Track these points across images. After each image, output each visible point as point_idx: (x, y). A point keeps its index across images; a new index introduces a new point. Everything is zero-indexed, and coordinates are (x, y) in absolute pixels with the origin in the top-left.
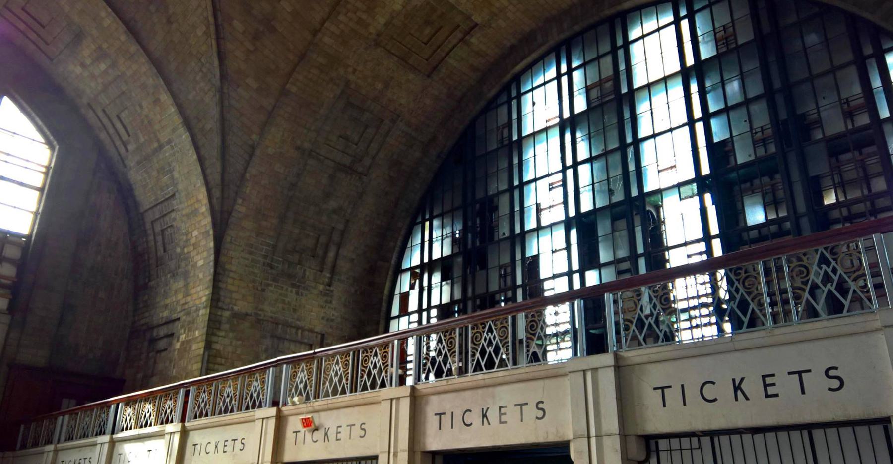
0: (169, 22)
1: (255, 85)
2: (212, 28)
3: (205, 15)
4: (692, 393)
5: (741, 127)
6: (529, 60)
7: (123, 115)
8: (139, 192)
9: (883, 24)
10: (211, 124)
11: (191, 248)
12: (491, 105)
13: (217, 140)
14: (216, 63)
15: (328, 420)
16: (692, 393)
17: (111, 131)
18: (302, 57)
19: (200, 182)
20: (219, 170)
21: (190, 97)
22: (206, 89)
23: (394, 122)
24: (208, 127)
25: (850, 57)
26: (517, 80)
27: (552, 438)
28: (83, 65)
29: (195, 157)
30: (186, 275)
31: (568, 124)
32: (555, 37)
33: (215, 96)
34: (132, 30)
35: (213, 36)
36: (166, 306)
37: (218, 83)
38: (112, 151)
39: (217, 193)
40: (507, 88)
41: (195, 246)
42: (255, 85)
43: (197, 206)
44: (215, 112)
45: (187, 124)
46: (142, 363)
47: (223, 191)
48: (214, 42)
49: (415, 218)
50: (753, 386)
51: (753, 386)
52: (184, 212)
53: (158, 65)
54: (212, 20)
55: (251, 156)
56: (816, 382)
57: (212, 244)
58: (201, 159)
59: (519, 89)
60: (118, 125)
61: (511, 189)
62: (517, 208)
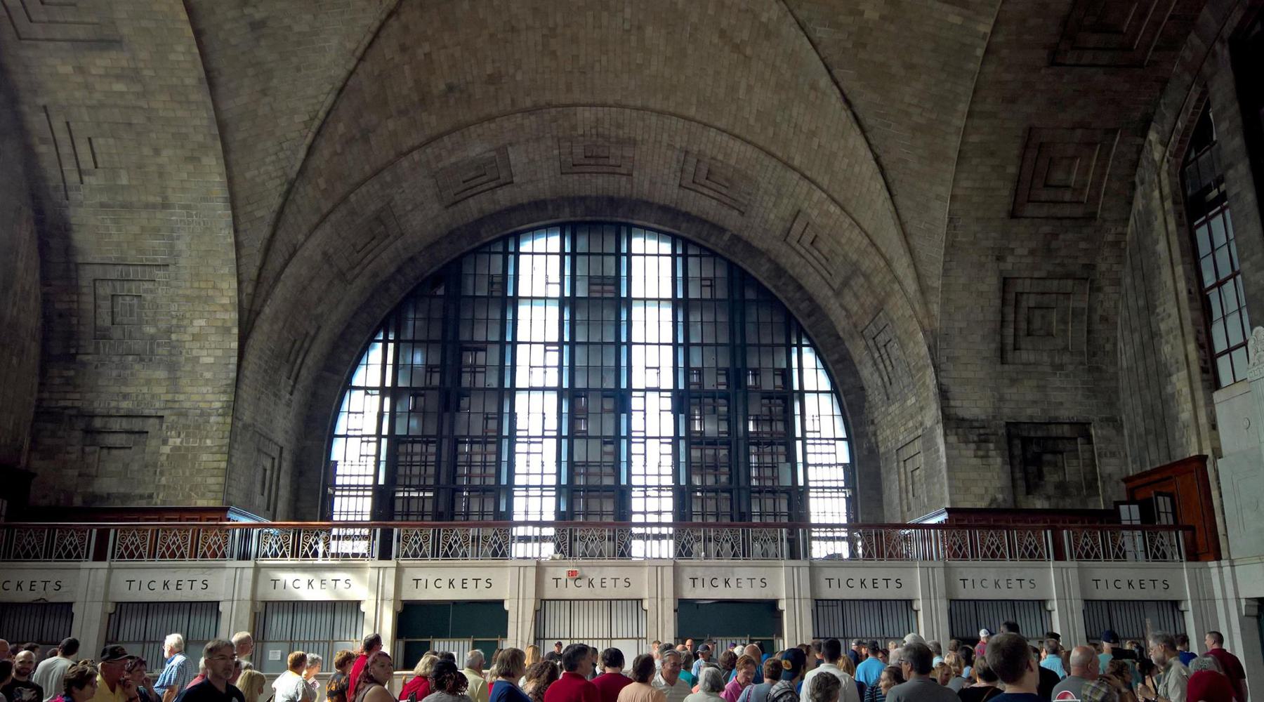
0: (264, 92)
1: (323, 186)
2: (317, 123)
3: (317, 107)
4: (843, 583)
5: (710, 362)
6: (535, 224)
7: (99, 143)
8: (82, 239)
9: (807, 330)
10: (265, 211)
11: (187, 337)
12: (484, 249)
13: (265, 231)
14: (302, 154)
15: (596, 575)
16: (843, 583)
17: (66, 149)
18: (377, 173)
19: (228, 270)
20: (258, 263)
21: (248, 175)
22: (274, 175)
23: (396, 239)
24: (259, 214)
25: (783, 341)
26: (517, 237)
27: (770, 597)
28: (80, 70)
29: (231, 240)
30: (172, 367)
31: (567, 302)
32: (566, 216)
33: (282, 185)
34: (211, 80)
35: (314, 129)
36: (126, 396)
37: (293, 175)
38: (52, 173)
39: (249, 289)
40: (505, 240)
41: (195, 337)
42: (323, 186)
43: (211, 293)
44: (276, 201)
45: (233, 201)
46: (74, 457)
47: (256, 288)
48: (310, 136)
49: (376, 333)
50: (869, 583)
51: (869, 583)
52: (180, 292)
53: (223, 127)
54: (322, 114)
55: (292, 256)
56: (892, 584)
57: (235, 345)
58: (238, 245)
59: (517, 246)
60: (83, 150)
61: (502, 343)
62: (508, 363)
